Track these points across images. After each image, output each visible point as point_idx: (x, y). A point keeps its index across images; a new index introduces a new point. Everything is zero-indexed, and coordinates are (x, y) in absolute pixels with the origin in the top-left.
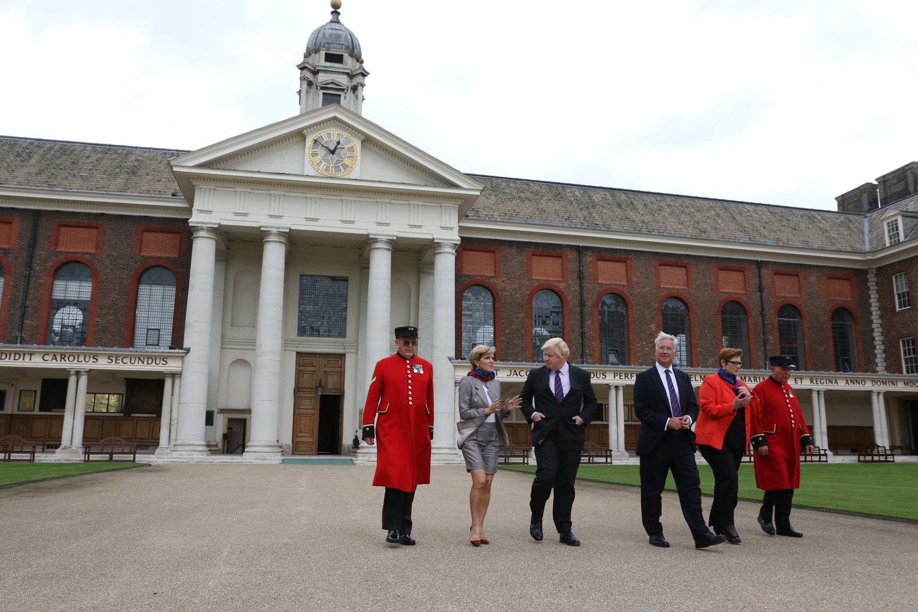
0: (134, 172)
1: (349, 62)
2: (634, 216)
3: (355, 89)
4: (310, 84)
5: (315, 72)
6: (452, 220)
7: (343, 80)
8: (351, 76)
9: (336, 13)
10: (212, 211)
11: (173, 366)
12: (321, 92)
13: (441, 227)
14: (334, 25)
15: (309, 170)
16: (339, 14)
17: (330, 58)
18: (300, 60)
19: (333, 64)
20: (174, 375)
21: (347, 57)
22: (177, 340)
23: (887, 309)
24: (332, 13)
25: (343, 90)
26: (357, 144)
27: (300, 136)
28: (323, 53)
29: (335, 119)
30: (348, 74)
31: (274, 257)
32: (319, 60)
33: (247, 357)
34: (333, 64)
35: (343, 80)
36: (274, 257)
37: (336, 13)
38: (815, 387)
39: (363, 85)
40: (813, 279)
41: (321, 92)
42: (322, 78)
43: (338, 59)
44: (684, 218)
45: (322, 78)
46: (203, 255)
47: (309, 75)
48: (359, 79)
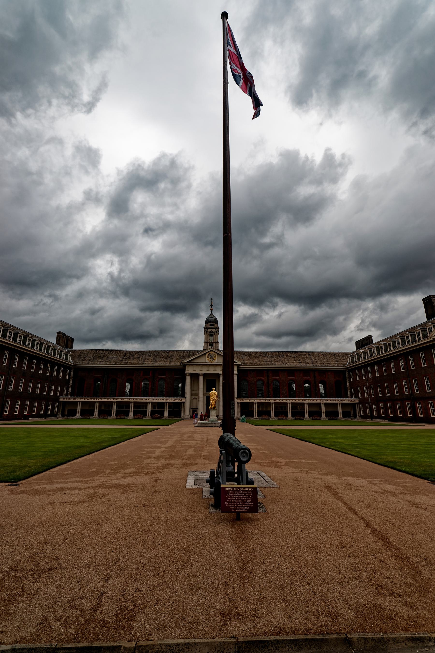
0: (171, 358)
2: (283, 359)
3: (216, 332)
5: (208, 329)
7: (214, 330)
8: (216, 329)
9: (212, 312)
10: (189, 370)
11: (183, 401)
15: (207, 361)
17: (211, 325)
20: (184, 403)
22: (183, 395)
23: (350, 380)
26: (216, 355)
27: (205, 354)
29: (212, 351)
31: (201, 378)
33: (197, 397)
35: (214, 330)
36: (201, 378)
37: (212, 312)
38: (321, 402)
40: (329, 373)
42: (209, 330)
43: (213, 325)
44: (296, 359)
45: (209, 330)
46: (188, 380)
47: (206, 330)
48: (217, 330)
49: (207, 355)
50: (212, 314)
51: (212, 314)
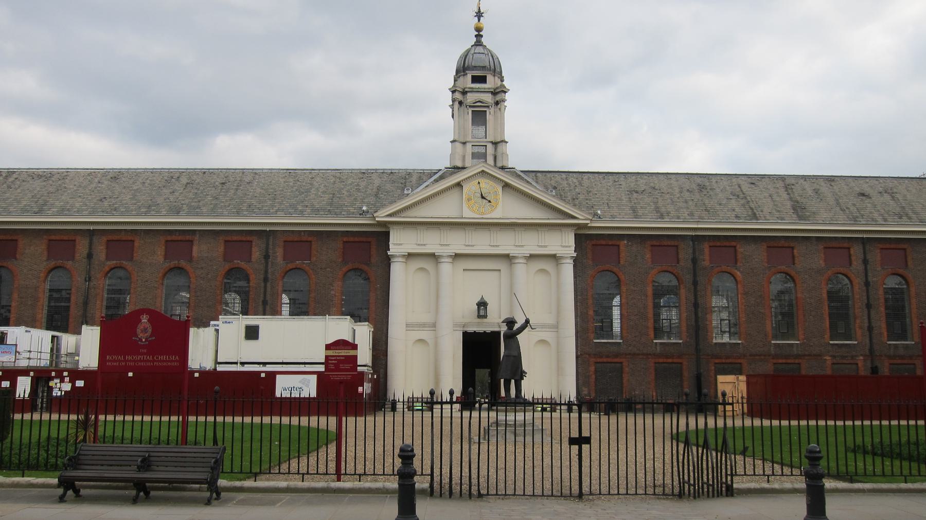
1: (492, 82)
3: (497, 103)
4: (461, 103)
5: (464, 93)
6: (570, 239)
7: (488, 98)
8: (494, 93)
9: (479, 36)
10: (400, 243)
12: (470, 110)
13: (564, 245)
14: (479, 49)
16: (482, 36)
17: (475, 79)
18: (451, 83)
19: (479, 83)
21: (490, 78)
24: (476, 36)
25: (488, 107)
26: (500, 189)
28: (469, 77)
29: (483, 171)
30: (492, 93)
32: (467, 82)
34: (479, 83)
35: (488, 98)
37: (479, 36)
39: (504, 101)
41: (470, 110)
42: (471, 98)
43: (482, 80)
45: (471, 98)
48: (498, 98)
49: (466, 188)
50: (478, 43)
51: (478, 43)
